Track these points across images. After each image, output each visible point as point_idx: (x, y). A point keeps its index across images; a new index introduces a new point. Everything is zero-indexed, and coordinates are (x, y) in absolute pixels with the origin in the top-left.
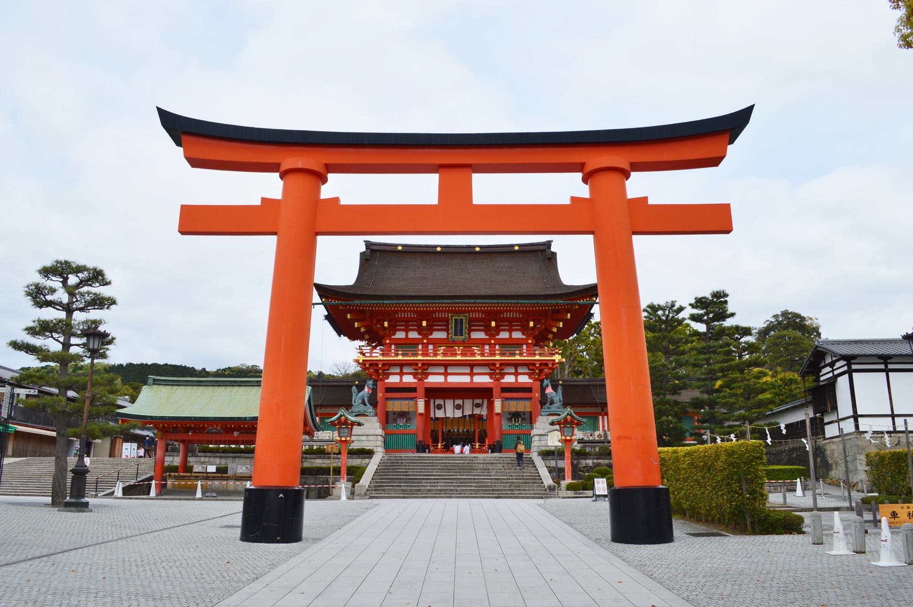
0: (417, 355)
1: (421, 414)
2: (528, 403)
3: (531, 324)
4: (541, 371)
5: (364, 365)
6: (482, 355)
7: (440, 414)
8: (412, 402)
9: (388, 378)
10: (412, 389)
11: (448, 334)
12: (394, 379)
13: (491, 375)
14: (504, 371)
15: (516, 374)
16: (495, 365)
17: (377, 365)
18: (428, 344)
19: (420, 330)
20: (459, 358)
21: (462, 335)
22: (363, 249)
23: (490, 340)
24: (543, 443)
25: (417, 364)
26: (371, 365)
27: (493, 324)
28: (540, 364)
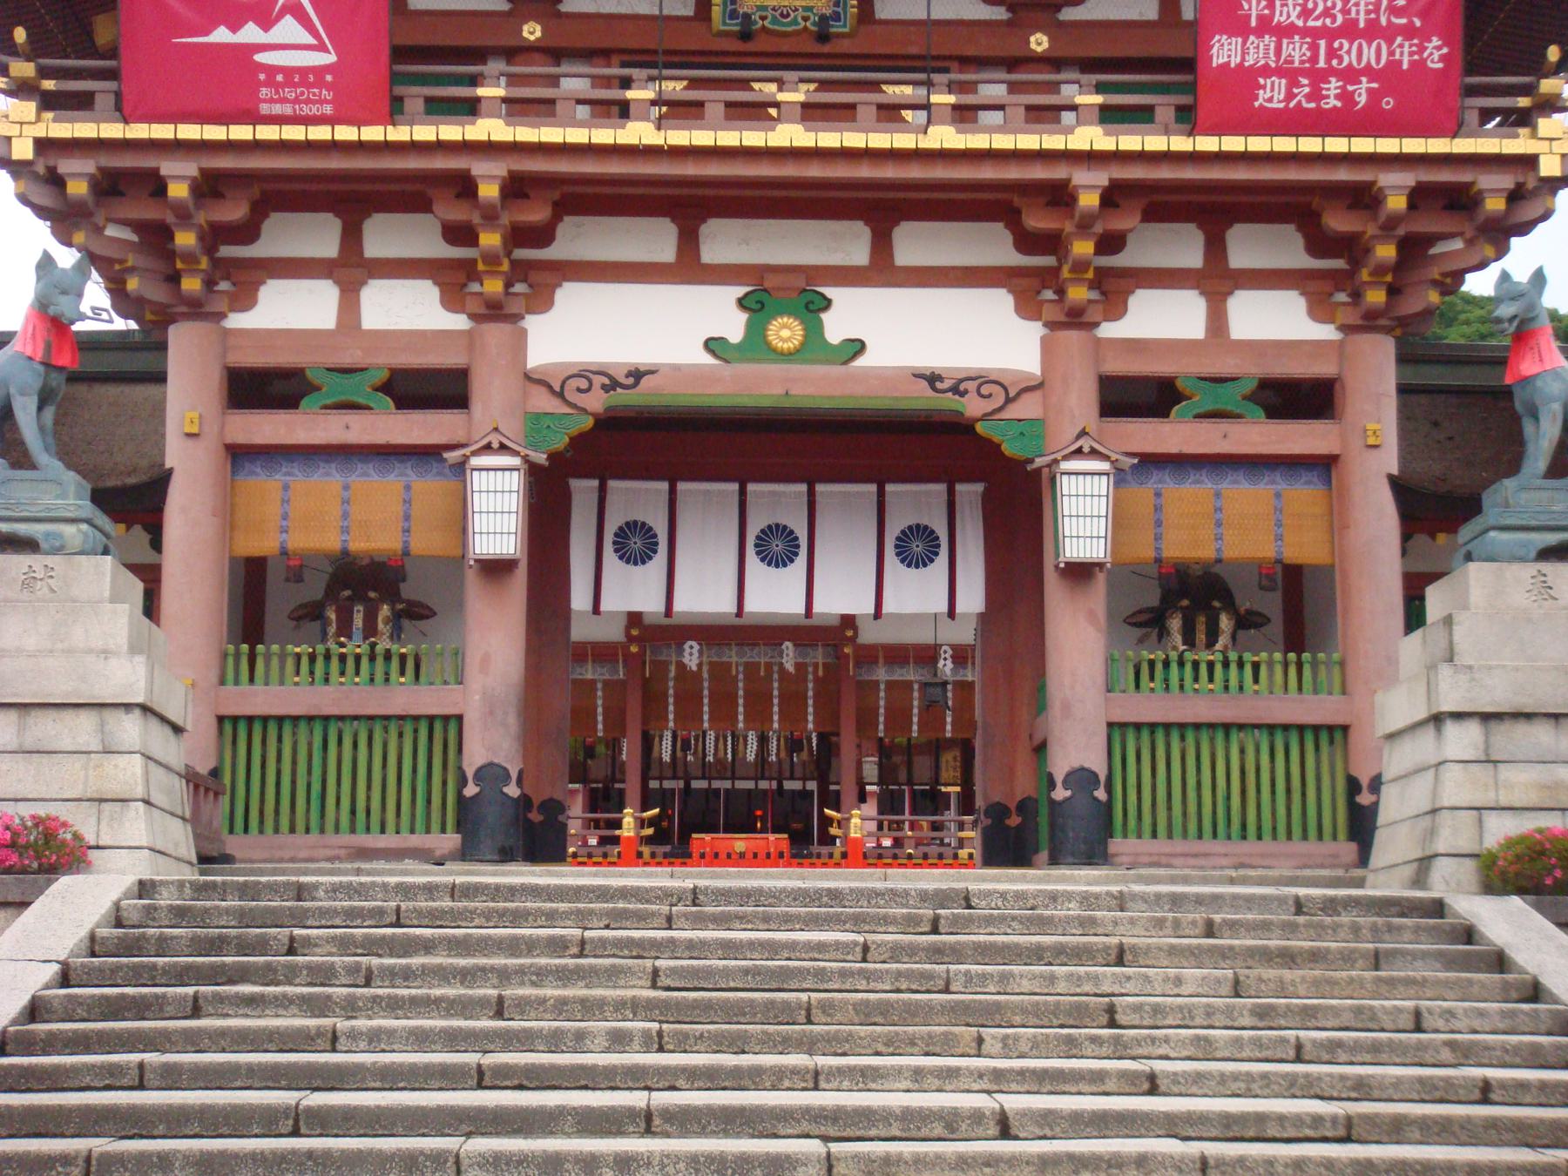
0: (471, 108)
1: (496, 569)
4: (1413, 248)
5: (56, 181)
7: (633, 591)
8: (427, 486)
9: (245, 299)
12: (292, 310)
13: (1028, 291)
15: (1216, 281)
16: (1060, 196)
17: (157, 185)
18: (554, 53)
23: (1019, 24)
24: (1520, 783)
25: (465, 186)
26: (110, 186)
28: (1419, 196)
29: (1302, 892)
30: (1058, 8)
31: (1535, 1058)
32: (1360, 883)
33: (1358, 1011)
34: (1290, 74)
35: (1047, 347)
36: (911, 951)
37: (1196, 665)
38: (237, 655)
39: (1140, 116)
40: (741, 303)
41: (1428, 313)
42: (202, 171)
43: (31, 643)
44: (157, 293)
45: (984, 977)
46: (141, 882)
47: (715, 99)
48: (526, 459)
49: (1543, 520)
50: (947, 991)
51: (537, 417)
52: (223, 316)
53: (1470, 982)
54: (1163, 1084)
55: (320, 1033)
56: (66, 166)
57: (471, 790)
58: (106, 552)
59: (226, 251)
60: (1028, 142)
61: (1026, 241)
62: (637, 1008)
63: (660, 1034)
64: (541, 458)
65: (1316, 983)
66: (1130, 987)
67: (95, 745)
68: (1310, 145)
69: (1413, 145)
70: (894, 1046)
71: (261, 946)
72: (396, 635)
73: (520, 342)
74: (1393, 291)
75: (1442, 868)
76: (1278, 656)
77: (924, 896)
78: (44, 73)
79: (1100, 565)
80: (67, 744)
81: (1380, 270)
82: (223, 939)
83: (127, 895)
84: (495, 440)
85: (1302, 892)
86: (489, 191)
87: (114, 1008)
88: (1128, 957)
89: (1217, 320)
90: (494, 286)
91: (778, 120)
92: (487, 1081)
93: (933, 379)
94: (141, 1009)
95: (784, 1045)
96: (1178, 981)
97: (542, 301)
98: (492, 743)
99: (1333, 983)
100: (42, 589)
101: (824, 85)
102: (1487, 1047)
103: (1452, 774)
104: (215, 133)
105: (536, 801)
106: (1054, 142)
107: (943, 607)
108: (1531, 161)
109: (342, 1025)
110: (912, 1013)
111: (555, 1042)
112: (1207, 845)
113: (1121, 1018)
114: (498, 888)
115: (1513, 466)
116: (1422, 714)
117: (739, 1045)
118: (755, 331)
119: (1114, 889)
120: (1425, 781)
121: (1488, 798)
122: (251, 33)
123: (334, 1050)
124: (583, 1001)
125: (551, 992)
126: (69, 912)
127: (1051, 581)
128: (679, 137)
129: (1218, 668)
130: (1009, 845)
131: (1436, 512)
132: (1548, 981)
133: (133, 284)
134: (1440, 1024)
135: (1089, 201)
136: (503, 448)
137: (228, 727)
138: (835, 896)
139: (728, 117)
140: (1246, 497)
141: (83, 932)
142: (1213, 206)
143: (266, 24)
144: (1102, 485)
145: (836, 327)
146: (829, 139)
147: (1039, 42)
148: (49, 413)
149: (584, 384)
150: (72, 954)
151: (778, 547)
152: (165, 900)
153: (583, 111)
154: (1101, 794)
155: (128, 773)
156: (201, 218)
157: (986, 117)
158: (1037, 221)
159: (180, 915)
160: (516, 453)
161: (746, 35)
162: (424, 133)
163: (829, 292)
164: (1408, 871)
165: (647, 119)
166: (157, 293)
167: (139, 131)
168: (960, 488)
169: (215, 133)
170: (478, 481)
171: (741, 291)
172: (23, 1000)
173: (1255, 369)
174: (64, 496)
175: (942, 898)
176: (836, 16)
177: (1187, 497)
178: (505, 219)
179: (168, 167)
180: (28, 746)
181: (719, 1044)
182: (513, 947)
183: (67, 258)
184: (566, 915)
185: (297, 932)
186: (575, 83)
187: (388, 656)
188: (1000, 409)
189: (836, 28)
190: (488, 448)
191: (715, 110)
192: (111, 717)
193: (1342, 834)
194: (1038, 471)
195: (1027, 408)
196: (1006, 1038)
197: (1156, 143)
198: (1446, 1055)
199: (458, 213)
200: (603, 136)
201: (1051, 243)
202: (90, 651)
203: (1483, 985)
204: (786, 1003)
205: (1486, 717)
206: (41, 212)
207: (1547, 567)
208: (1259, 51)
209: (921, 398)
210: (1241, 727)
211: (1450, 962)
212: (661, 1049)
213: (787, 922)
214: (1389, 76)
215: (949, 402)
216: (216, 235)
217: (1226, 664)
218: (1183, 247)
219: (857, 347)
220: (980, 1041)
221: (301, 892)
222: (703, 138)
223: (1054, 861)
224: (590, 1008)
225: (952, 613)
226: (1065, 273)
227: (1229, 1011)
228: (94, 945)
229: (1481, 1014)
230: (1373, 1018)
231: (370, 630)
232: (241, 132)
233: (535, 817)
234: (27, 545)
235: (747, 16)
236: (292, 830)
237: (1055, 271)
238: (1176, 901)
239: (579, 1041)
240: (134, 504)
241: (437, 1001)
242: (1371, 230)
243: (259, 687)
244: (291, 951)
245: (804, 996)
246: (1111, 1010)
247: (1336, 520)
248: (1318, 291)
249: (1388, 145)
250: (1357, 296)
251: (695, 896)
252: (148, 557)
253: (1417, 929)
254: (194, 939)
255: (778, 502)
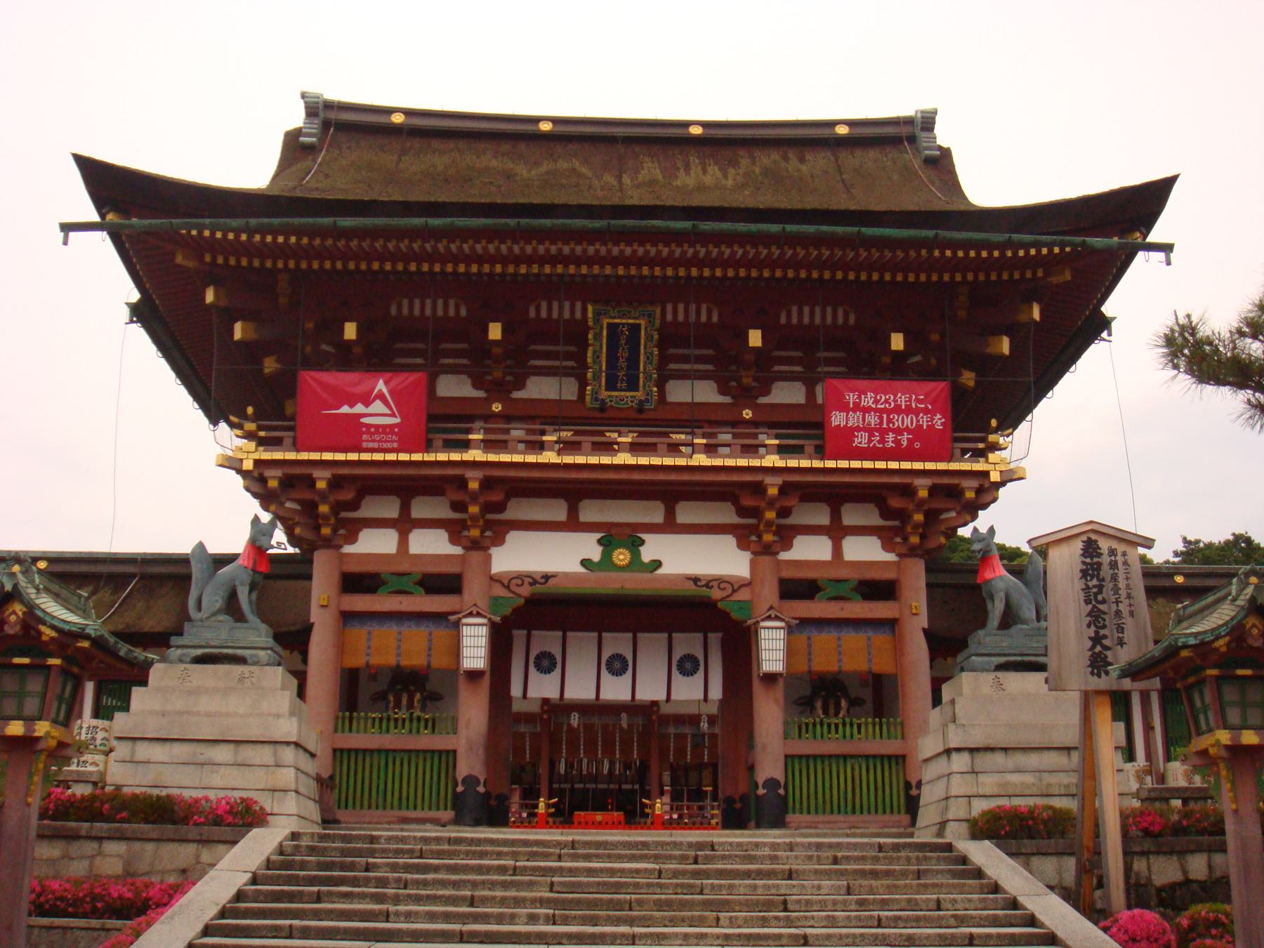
0: (466, 445)
1: (474, 675)
2: (881, 639)
3: (897, 342)
5: (263, 480)
6: (710, 449)
7: (544, 687)
8: (441, 634)
9: (352, 539)
10: (444, 582)
11: (583, 384)
12: (375, 544)
13: (744, 536)
14: (793, 520)
15: (837, 532)
16: (758, 489)
17: (312, 482)
18: (506, 417)
19: (478, 361)
20: (624, 458)
21: (633, 386)
22: (296, 118)
23: (738, 405)
24: (988, 783)
25: (462, 483)
26: (288, 482)
27: (755, 338)
28: (933, 490)
29: (882, 840)
30: (757, 398)
31: (995, 922)
32: (911, 835)
33: (909, 901)
34: (870, 431)
35: (753, 564)
36: (683, 873)
37: (829, 725)
38: (344, 718)
39: (796, 451)
40: (600, 542)
41: (941, 547)
42: (333, 475)
43: (241, 710)
44: (309, 535)
45: (720, 886)
46: (293, 833)
47: (587, 440)
48: (490, 619)
49: (998, 651)
50: (701, 893)
51: (496, 598)
52: (341, 547)
53: (964, 885)
54: (811, 940)
55: (380, 912)
56: (268, 473)
57: (460, 789)
58: (279, 665)
59: (344, 514)
60: (742, 462)
61: (741, 511)
62: (542, 902)
63: (554, 915)
64: (497, 619)
65: (888, 887)
66: (795, 891)
67: (271, 762)
68: (880, 465)
69: (930, 466)
70: (673, 922)
71: (352, 867)
72: (423, 709)
73: (488, 561)
74: (923, 537)
75: (951, 827)
76: (870, 720)
77: (690, 845)
78: (260, 428)
79: (781, 675)
80: (258, 762)
81: (916, 526)
82: (333, 863)
83: (286, 839)
84: (475, 610)
85: (882, 840)
86: (474, 485)
87: (277, 897)
88: (794, 875)
89: (837, 551)
90: (475, 533)
91: (618, 451)
92: (465, 938)
93: (695, 580)
94: (291, 897)
95: (618, 921)
96: (819, 887)
97: (499, 540)
98: (470, 764)
99: (895, 886)
100: (248, 683)
101: (641, 434)
102: (972, 917)
103: (956, 779)
104: (340, 457)
105: (494, 795)
106: (755, 463)
107: (702, 697)
108: (986, 474)
109: (392, 908)
110: (683, 905)
111: (500, 919)
112: (835, 817)
113: (790, 906)
114: (472, 839)
115: (982, 624)
116: (941, 749)
117: (594, 921)
118: (606, 555)
119: (787, 840)
120: (943, 782)
121: (973, 791)
122: (360, 408)
123: (387, 921)
124: (515, 899)
125: (499, 893)
126: (256, 848)
127: (756, 683)
128: (569, 459)
129: (840, 727)
130: (734, 820)
131: (947, 647)
132: (1002, 883)
133: (298, 531)
134: (950, 906)
135: (773, 491)
136: (479, 615)
137: (338, 754)
138: (645, 845)
139: (593, 450)
140: (853, 640)
141: (264, 858)
142: (835, 494)
143: (367, 405)
144: (781, 634)
145: (647, 554)
146: (643, 461)
147: (747, 414)
148: (254, 595)
149: (519, 582)
150: (258, 868)
151: (618, 666)
152: (305, 842)
153: (521, 446)
154: (781, 791)
155: (287, 777)
156: (332, 498)
157: (722, 450)
158: (748, 502)
159: (312, 850)
160: (484, 617)
161: (603, 409)
162: (442, 457)
163: (643, 536)
164: (935, 829)
165: (552, 450)
166: (309, 535)
167: (304, 456)
168: (710, 635)
169: (340, 457)
170: (466, 631)
171: (599, 535)
172: (233, 891)
173: (855, 575)
174: (259, 636)
175: (700, 846)
176: (647, 401)
177: (824, 639)
178: (482, 500)
179: (317, 473)
180: (240, 759)
181: (585, 921)
182: (480, 870)
183: (266, 517)
184: (507, 854)
185: (371, 860)
186: (517, 433)
187: (419, 719)
188: (730, 595)
189: (647, 406)
190: (471, 615)
191: (587, 446)
192: (280, 748)
193: (903, 811)
194: (749, 627)
195: (743, 595)
196: (731, 917)
197: (805, 463)
198: (952, 922)
199: (458, 496)
200: (531, 458)
201: (756, 513)
202: (270, 714)
203: (970, 885)
204: (619, 900)
205: (972, 750)
206: (255, 495)
207: (1000, 674)
208: (854, 419)
209: (690, 588)
210: (852, 756)
211: (955, 875)
212: (554, 924)
213: (620, 858)
214: (917, 432)
215: (704, 591)
216: (338, 507)
217: (844, 724)
218: (822, 517)
219: (657, 564)
220: (718, 919)
221: (373, 839)
222: (580, 460)
223: (758, 826)
224: (518, 902)
225: (706, 699)
226: (762, 527)
227: (845, 902)
228: (269, 864)
229: (970, 900)
230: (917, 904)
231: (410, 706)
232: (353, 456)
233: (493, 802)
234: (241, 660)
235: (603, 400)
236: (370, 807)
237: (757, 526)
238: (819, 846)
239: (512, 919)
240: (293, 641)
241: (440, 897)
242: (911, 507)
243: (354, 734)
244: (367, 870)
245: (628, 897)
246: (785, 902)
247: (898, 649)
248: (887, 538)
249: (918, 466)
250: (905, 539)
251: (573, 844)
252: (300, 667)
253: (938, 858)
254: (319, 863)
255: (617, 643)
